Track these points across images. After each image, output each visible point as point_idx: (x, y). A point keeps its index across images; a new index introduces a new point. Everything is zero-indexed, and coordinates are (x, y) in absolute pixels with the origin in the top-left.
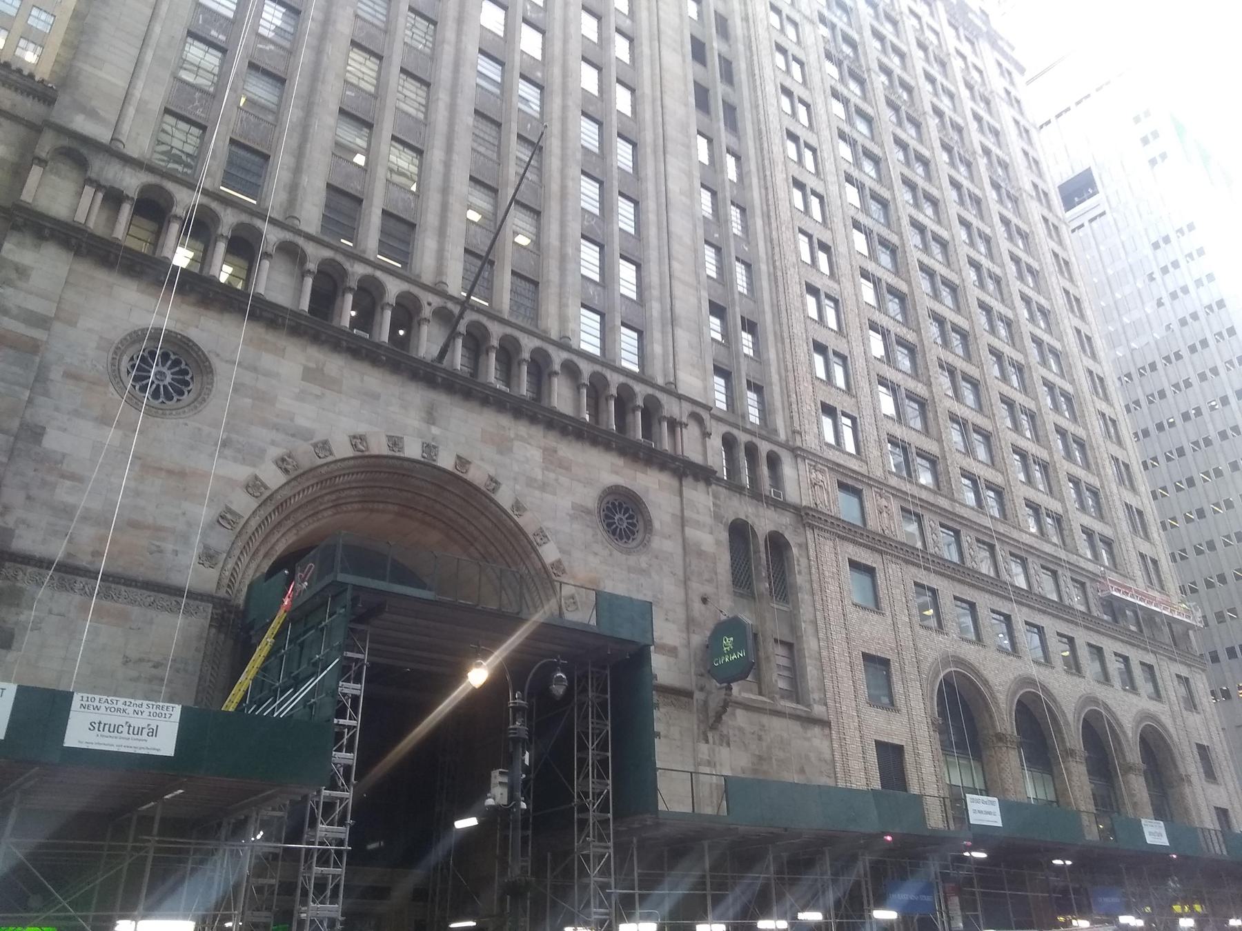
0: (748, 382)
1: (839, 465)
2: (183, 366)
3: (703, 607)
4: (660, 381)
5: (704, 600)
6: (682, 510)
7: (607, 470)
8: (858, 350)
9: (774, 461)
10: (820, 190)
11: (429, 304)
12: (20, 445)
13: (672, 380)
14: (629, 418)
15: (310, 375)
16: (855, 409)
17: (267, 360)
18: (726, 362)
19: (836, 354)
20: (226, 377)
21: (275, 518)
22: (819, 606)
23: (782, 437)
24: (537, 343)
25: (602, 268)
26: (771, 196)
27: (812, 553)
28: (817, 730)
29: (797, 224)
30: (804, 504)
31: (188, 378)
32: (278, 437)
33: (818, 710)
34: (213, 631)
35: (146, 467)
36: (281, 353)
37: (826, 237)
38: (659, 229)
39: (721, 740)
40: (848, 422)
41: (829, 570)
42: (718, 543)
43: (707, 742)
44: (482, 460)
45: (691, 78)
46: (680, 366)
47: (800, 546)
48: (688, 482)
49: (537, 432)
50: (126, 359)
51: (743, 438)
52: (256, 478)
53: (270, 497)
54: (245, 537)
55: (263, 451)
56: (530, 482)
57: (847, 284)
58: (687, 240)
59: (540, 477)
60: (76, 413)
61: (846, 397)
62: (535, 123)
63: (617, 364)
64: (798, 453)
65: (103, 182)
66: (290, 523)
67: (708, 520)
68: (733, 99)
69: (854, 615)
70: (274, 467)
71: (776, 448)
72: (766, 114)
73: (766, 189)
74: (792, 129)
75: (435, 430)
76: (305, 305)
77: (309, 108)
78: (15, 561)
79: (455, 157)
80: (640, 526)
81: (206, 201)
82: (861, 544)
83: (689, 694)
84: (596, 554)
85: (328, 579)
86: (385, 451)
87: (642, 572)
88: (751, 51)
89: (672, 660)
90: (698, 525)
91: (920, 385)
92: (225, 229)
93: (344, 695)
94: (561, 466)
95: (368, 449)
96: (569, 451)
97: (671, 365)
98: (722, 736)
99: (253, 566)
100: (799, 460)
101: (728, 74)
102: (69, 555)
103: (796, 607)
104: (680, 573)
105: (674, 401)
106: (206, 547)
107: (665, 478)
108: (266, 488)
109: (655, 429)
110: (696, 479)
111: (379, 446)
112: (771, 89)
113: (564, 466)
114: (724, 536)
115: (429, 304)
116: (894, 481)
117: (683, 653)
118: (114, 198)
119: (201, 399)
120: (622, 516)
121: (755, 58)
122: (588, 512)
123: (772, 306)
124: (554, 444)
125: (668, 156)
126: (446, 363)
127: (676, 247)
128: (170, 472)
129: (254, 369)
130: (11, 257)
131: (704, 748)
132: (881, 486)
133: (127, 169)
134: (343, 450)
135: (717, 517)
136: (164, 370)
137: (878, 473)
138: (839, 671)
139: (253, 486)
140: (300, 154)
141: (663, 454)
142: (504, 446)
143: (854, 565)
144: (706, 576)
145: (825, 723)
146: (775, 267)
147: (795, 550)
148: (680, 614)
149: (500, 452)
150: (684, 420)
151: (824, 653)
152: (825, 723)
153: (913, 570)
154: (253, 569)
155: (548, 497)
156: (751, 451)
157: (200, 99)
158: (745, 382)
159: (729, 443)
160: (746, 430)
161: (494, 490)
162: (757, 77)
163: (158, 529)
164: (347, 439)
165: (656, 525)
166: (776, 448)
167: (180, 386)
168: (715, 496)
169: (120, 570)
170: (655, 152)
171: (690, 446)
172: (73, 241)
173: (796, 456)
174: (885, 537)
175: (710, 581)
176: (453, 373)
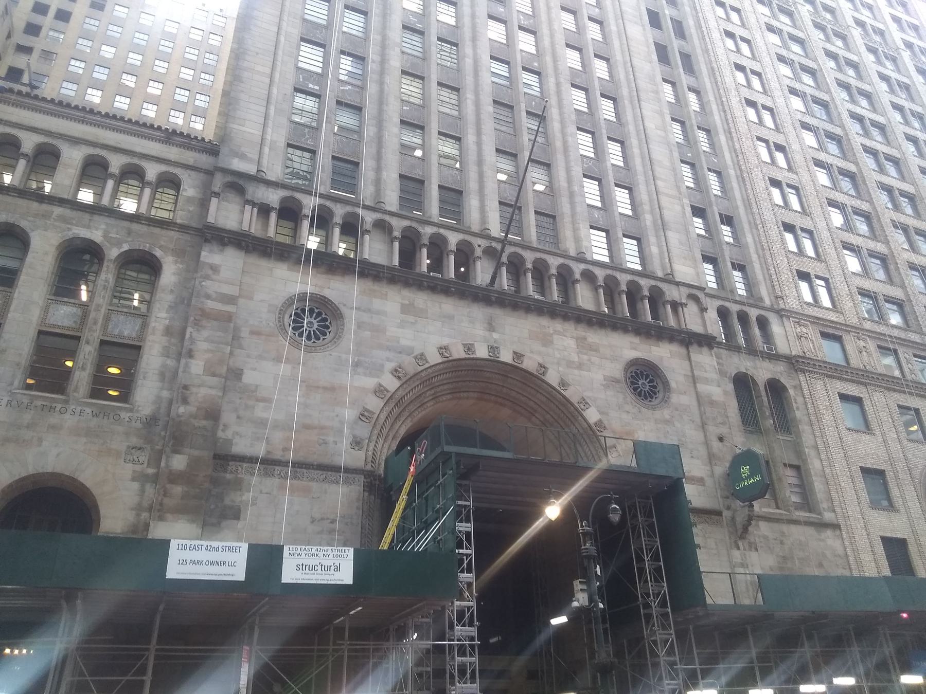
0: (733, 264)
1: (818, 318)
2: (324, 316)
3: (720, 444)
4: (660, 274)
5: (721, 439)
6: (692, 371)
8: (821, 225)
9: (763, 323)
10: (769, 104)
11: (479, 246)
12: (228, 383)
13: (669, 271)
14: (639, 305)
15: (406, 309)
16: (825, 271)
17: (377, 304)
18: (711, 251)
19: (803, 230)
20: (352, 318)
21: (396, 411)
22: (818, 434)
23: (767, 302)
24: (561, 261)
25: (602, 196)
26: (729, 117)
27: (806, 392)
28: (829, 532)
29: (754, 133)
30: (794, 353)
31: (327, 323)
32: (391, 355)
33: (828, 516)
34: (366, 494)
35: (310, 387)
36: (384, 297)
37: (780, 139)
38: (643, 158)
39: (750, 547)
40: (822, 283)
41: (822, 404)
42: (726, 393)
43: (738, 548)
44: (532, 352)
45: (651, 41)
46: (675, 259)
47: (795, 387)
48: (694, 349)
49: (569, 327)
50: (287, 316)
51: (734, 308)
52: (380, 385)
53: (391, 397)
54: (379, 427)
55: (382, 366)
56: (570, 364)
57: (804, 173)
58: (667, 163)
59: (576, 359)
60: (260, 357)
61: (817, 264)
62: (537, 100)
63: (624, 267)
64: (782, 314)
65: (256, 201)
66: (406, 414)
67: (714, 376)
68: (687, 49)
69: (849, 438)
70: (391, 376)
71: (763, 313)
72: (715, 55)
73: (725, 111)
74: (738, 62)
75: (495, 336)
76: (396, 262)
77: (380, 124)
78: (235, 461)
79: (484, 137)
80: (660, 387)
81: (323, 201)
82: (847, 380)
83: (719, 513)
84: (628, 412)
85: (438, 450)
86: (463, 355)
87: (667, 422)
88: (696, 10)
89: (701, 488)
90: (707, 381)
91: (879, 244)
92: (338, 219)
93: (460, 532)
94: (591, 350)
95: (451, 356)
96: (596, 337)
97: (667, 260)
98: (750, 544)
99: (386, 446)
100: (784, 319)
101: (680, 30)
102: (269, 452)
103: (798, 435)
104: (698, 420)
105: (673, 287)
106: (354, 437)
107: (675, 348)
108: (388, 391)
109: (661, 311)
110: (700, 345)
111: (458, 353)
112: (716, 35)
113: (593, 349)
114: (730, 387)
115: (479, 246)
116: (868, 325)
117: (709, 482)
118: (264, 210)
119: (338, 337)
120: (645, 382)
121: (700, 14)
122: (617, 381)
123: (743, 200)
124: (584, 334)
125: (642, 103)
126: (496, 285)
127: (658, 171)
128: (325, 388)
129: (369, 311)
130: (207, 261)
131: (736, 554)
132: (858, 331)
133: (270, 190)
134: (434, 358)
135: (722, 373)
136: (312, 320)
137: (854, 321)
138: (843, 484)
139: (379, 391)
140: (379, 158)
141: (671, 329)
142: (547, 341)
143: (844, 397)
144: (720, 420)
145: (836, 527)
146: (741, 170)
147: (791, 392)
148: (703, 451)
149: (544, 345)
150: (684, 301)
151: (827, 470)
152: (836, 527)
153: (896, 395)
154: (386, 449)
155: (585, 373)
156: (743, 318)
157: (309, 132)
158: (729, 264)
159: (723, 314)
160: (736, 302)
161: (544, 374)
162: (704, 29)
163: (322, 428)
164: (436, 351)
165: (673, 385)
166: (763, 313)
167: (324, 329)
168: (718, 357)
169: (302, 459)
170: (631, 102)
171: (691, 320)
172: (243, 244)
173: (781, 316)
174: (867, 372)
175: (723, 423)
176: (502, 293)
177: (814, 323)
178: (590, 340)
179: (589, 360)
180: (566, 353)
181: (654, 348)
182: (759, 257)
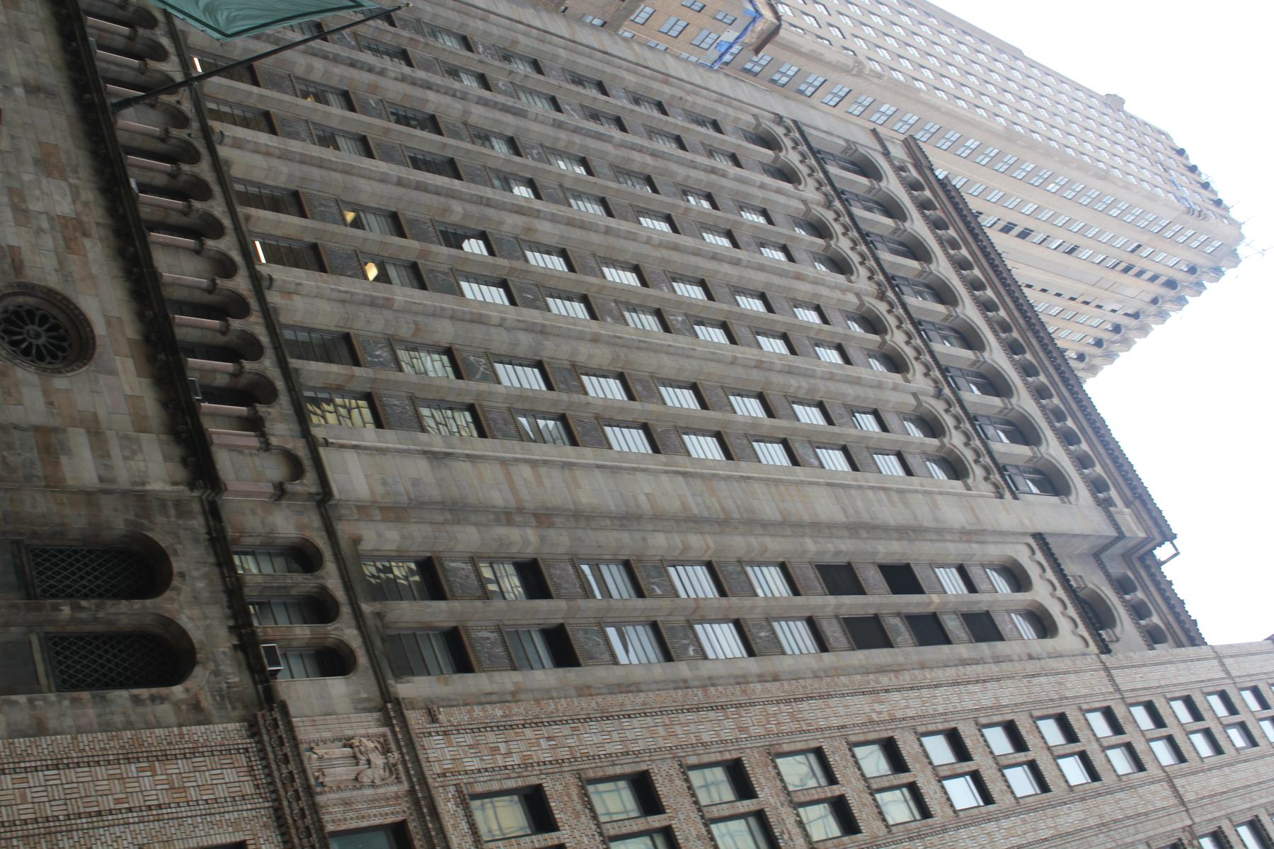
7: (103, 302)
9: (332, 661)
42: (89, 496)
44: (13, 137)
80: (43, 365)
100: (376, 715)
113: (70, 244)
114: (117, 521)
122: (18, 267)
125: (680, 479)
142: (46, 164)
147: (178, 691)
150: (274, 441)
165: (60, 382)
168: (178, 504)
177: (416, 802)
178: (87, 243)
179: (40, 230)
180: (37, 192)
181: (130, 363)
182: (513, 693)
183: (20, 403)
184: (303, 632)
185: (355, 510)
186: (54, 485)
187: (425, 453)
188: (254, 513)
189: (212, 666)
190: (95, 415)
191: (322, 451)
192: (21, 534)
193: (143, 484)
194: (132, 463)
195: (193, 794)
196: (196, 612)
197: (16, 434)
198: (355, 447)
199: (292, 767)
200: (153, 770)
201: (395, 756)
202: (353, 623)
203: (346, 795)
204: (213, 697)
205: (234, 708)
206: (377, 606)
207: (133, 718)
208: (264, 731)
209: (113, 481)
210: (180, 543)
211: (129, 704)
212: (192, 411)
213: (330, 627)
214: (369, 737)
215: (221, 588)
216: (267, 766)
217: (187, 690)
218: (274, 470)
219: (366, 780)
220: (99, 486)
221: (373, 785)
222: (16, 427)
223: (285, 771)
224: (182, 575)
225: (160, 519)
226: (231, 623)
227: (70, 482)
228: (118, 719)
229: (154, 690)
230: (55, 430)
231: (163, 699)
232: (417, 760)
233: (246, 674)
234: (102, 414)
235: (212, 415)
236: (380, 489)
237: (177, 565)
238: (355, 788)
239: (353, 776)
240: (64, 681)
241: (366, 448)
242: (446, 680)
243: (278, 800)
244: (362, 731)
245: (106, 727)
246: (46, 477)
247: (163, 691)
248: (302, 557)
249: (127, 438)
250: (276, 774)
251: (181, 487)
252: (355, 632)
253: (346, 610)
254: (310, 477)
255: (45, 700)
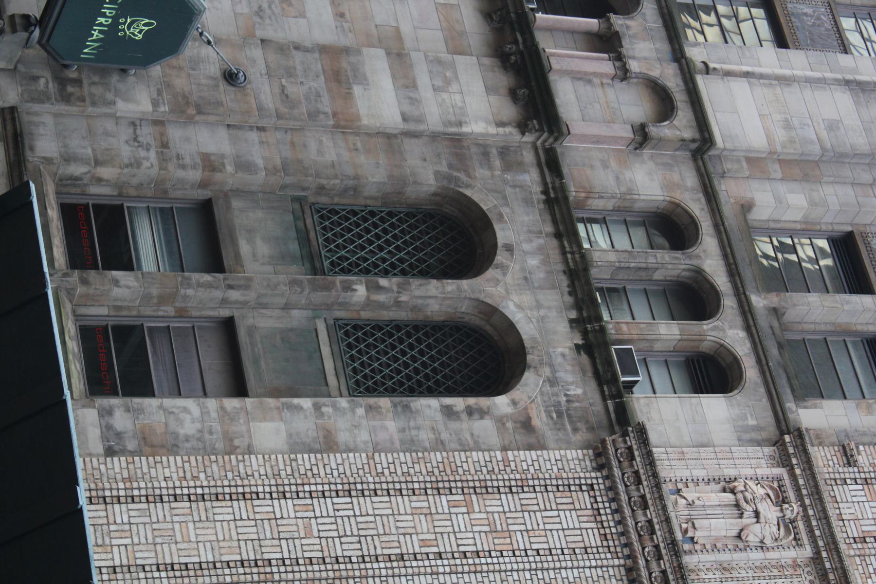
3: (214, 70)
5: (230, 77)
9: (710, 373)
27: (525, 458)
42: (390, 140)
90: (405, 81)
100: (768, 450)
114: (425, 174)
147: (502, 403)
150: (634, 66)
175: (284, 94)
183: (302, 15)
184: (669, 331)
185: (745, 164)
186: (345, 125)
187: (847, 83)
188: (605, 166)
189: (546, 371)
190: (397, 30)
191: (700, 80)
192: (304, 189)
193: (460, 124)
194: (445, 96)
195: (520, 541)
196: (527, 299)
197: (298, 56)
198: (747, 75)
199: (651, 513)
200: (469, 505)
201: (793, 510)
202: (739, 320)
203: (724, 557)
204: (548, 413)
205: (575, 430)
206: (773, 299)
207: (445, 436)
208: (614, 463)
209: (420, 120)
210: (507, 205)
211: (439, 416)
212: (525, 26)
213: (706, 326)
214: (758, 480)
215: (560, 267)
216: (618, 511)
217: (514, 403)
218: (634, 106)
219: (753, 540)
220: (402, 126)
221: (762, 546)
222: (297, 48)
223: (641, 518)
224: (509, 248)
225: (481, 172)
226: (573, 315)
227: (365, 121)
228: (425, 436)
229: (472, 401)
230: (346, 51)
231: (483, 413)
232: (825, 517)
233: (593, 385)
234: (406, 29)
235: (550, 29)
236: (780, 135)
237: (503, 235)
238: (736, 549)
239: (734, 533)
240: (357, 383)
241: (761, 76)
242: (869, 407)
243: (632, 556)
244: (749, 472)
245: (410, 445)
246: (335, 115)
247: (484, 402)
248: (671, 228)
249: (439, 62)
250: (630, 522)
251: (508, 129)
252: (742, 334)
253: (729, 302)
254: (683, 117)
255: (334, 406)
